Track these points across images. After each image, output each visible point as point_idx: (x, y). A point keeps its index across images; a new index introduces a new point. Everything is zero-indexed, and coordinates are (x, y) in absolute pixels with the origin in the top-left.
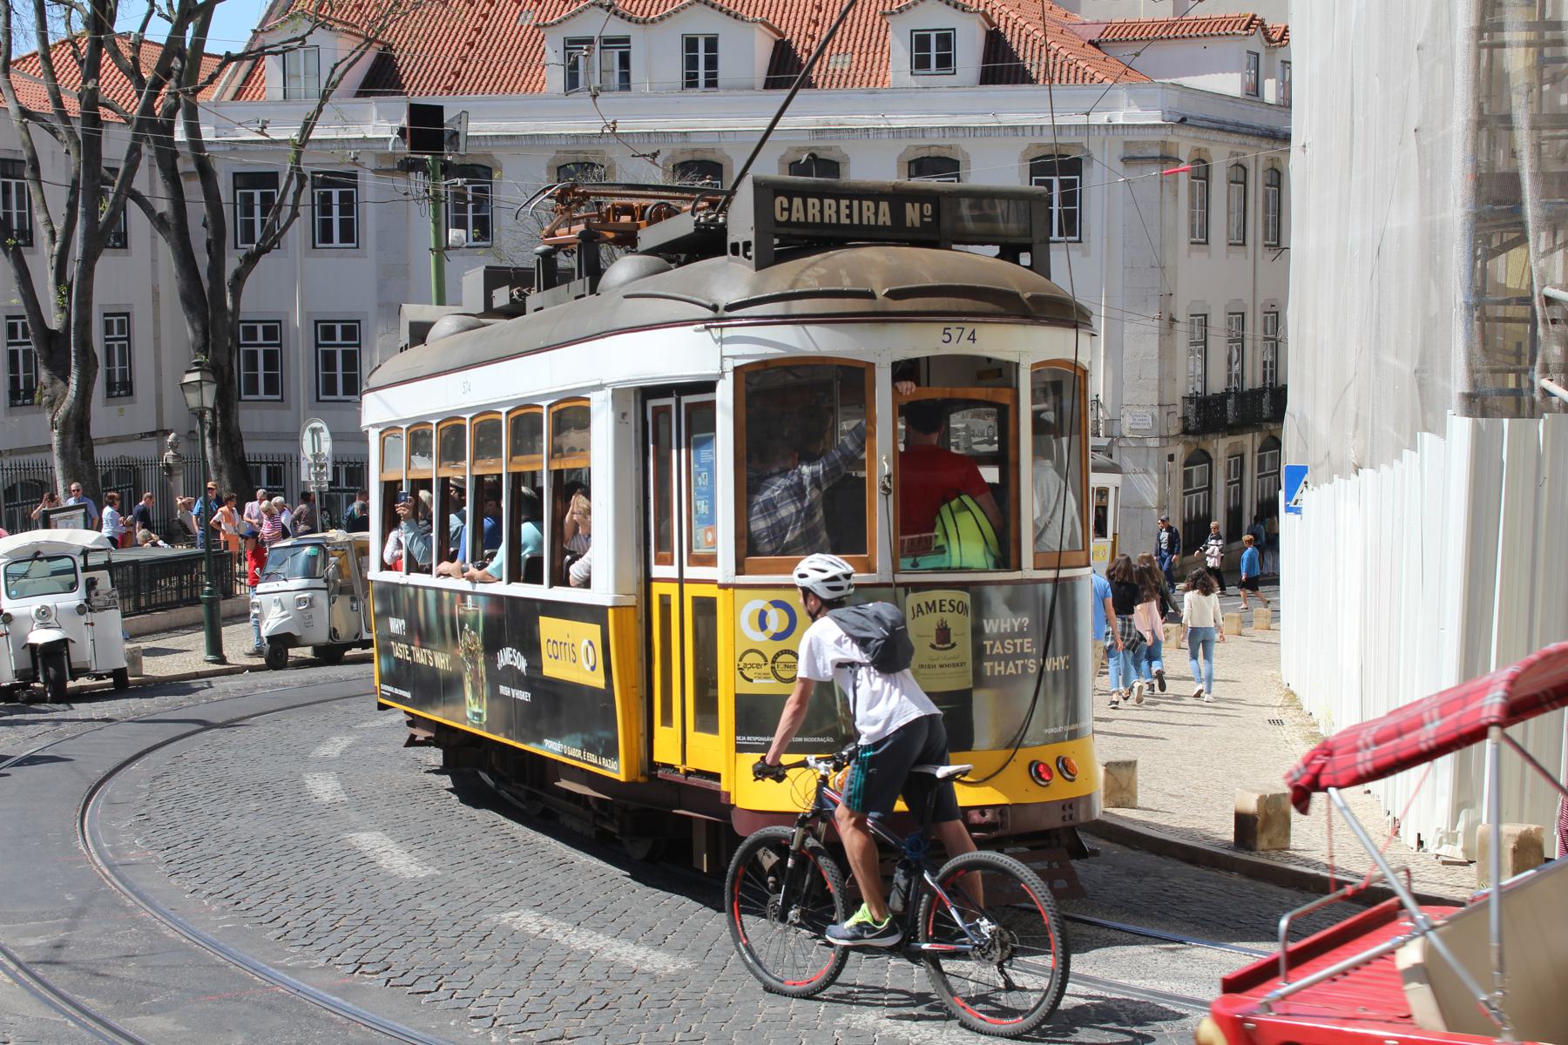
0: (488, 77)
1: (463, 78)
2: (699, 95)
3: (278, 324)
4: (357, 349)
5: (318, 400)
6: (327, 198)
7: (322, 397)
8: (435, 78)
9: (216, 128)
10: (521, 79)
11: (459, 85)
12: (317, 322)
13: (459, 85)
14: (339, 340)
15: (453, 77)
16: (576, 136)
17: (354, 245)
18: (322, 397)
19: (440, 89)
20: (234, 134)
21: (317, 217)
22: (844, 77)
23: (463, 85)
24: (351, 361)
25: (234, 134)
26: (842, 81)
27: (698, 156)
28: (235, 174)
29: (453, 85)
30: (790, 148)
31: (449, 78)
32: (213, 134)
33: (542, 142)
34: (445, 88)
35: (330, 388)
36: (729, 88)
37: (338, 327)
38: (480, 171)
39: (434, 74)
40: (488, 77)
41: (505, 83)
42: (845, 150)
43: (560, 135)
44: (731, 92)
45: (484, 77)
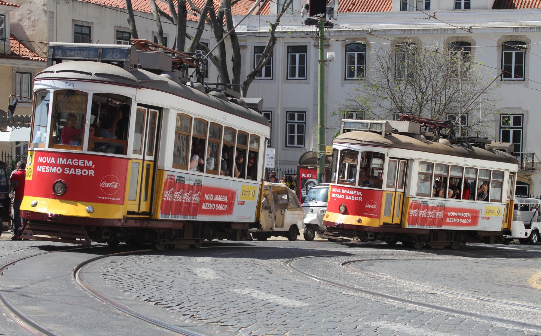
0: (367, 5)
1: (356, 6)
2: (462, 12)
3: (270, 113)
4: (304, 124)
5: (286, 146)
6: (294, 58)
7: (288, 145)
8: (344, 6)
9: (248, 27)
10: (382, 6)
11: (354, 9)
12: (287, 112)
13: (354, 9)
14: (296, 120)
15: (352, 5)
16: (405, 30)
17: (305, 78)
18: (288, 145)
19: (345, 10)
20: (255, 29)
21: (289, 66)
22: (530, 4)
23: (356, 9)
24: (301, 129)
25: (255, 29)
26: (529, 6)
27: (460, 40)
28: (255, 47)
29: (351, 9)
30: (503, 36)
31: (350, 6)
32: (246, 29)
33: (389, 33)
34: (348, 10)
35: (292, 141)
36: (475, 9)
37: (296, 114)
38: (360, 46)
39: (343, 4)
40: (367, 5)
41: (374, 8)
42: (528, 37)
43: (397, 30)
44: (476, 11)
45: (365, 5)
